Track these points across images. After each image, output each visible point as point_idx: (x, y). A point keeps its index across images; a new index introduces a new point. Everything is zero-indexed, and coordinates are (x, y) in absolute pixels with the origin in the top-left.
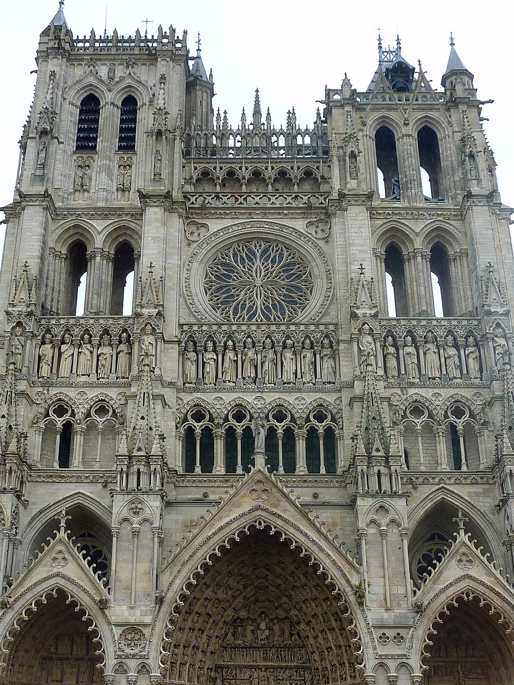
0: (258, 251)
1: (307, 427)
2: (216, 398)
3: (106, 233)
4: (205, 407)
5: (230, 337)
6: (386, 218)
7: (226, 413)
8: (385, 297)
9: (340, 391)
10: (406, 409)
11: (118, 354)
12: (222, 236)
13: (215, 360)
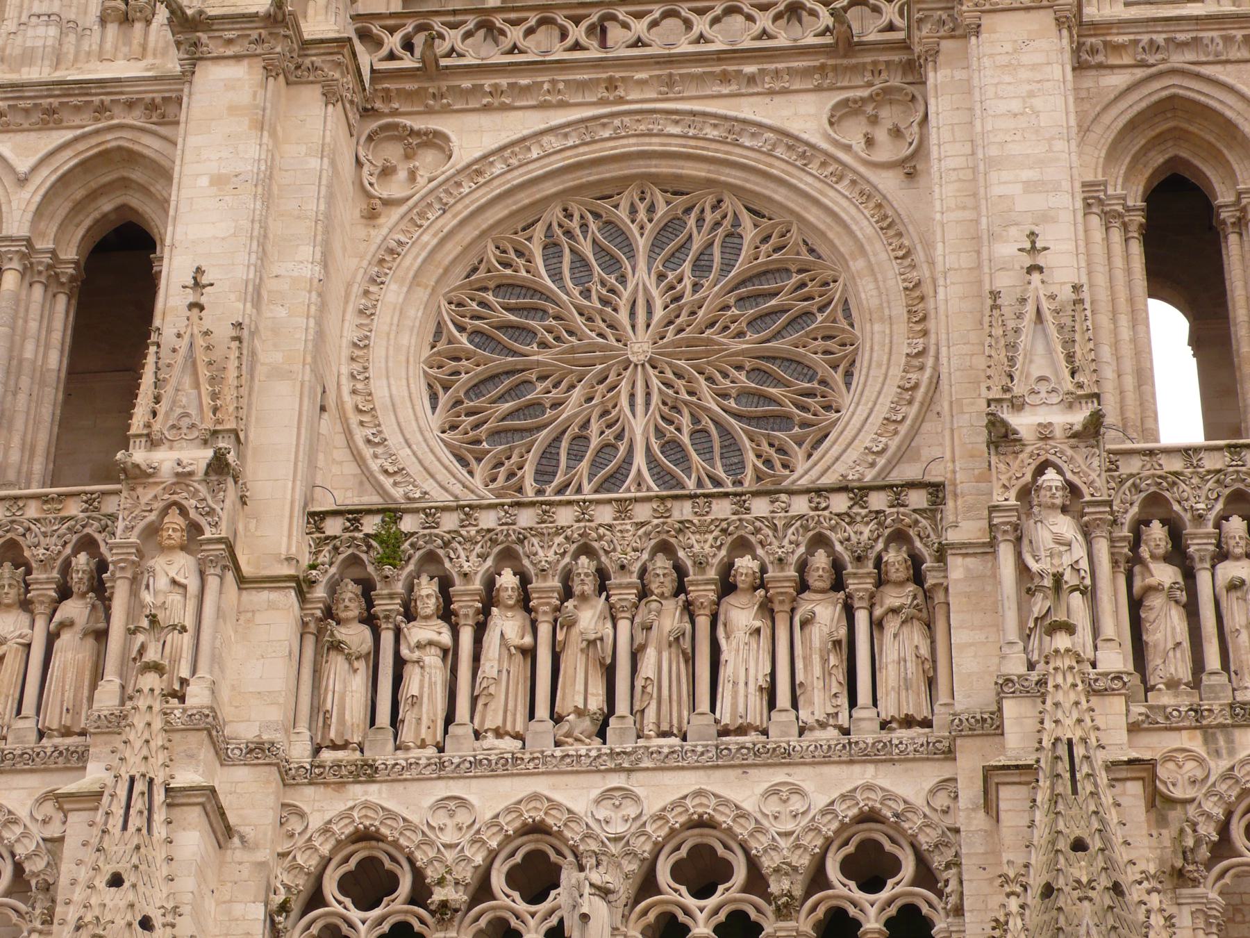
0: (642, 228)
1: (814, 909)
2: (442, 804)
3: (45, 178)
4: (395, 844)
5: (508, 556)
6: (1143, 64)
7: (479, 859)
8: (1144, 376)
9: (949, 754)
10: (1229, 814)
11: (51, 638)
12: (501, 177)
13: (445, 651)
